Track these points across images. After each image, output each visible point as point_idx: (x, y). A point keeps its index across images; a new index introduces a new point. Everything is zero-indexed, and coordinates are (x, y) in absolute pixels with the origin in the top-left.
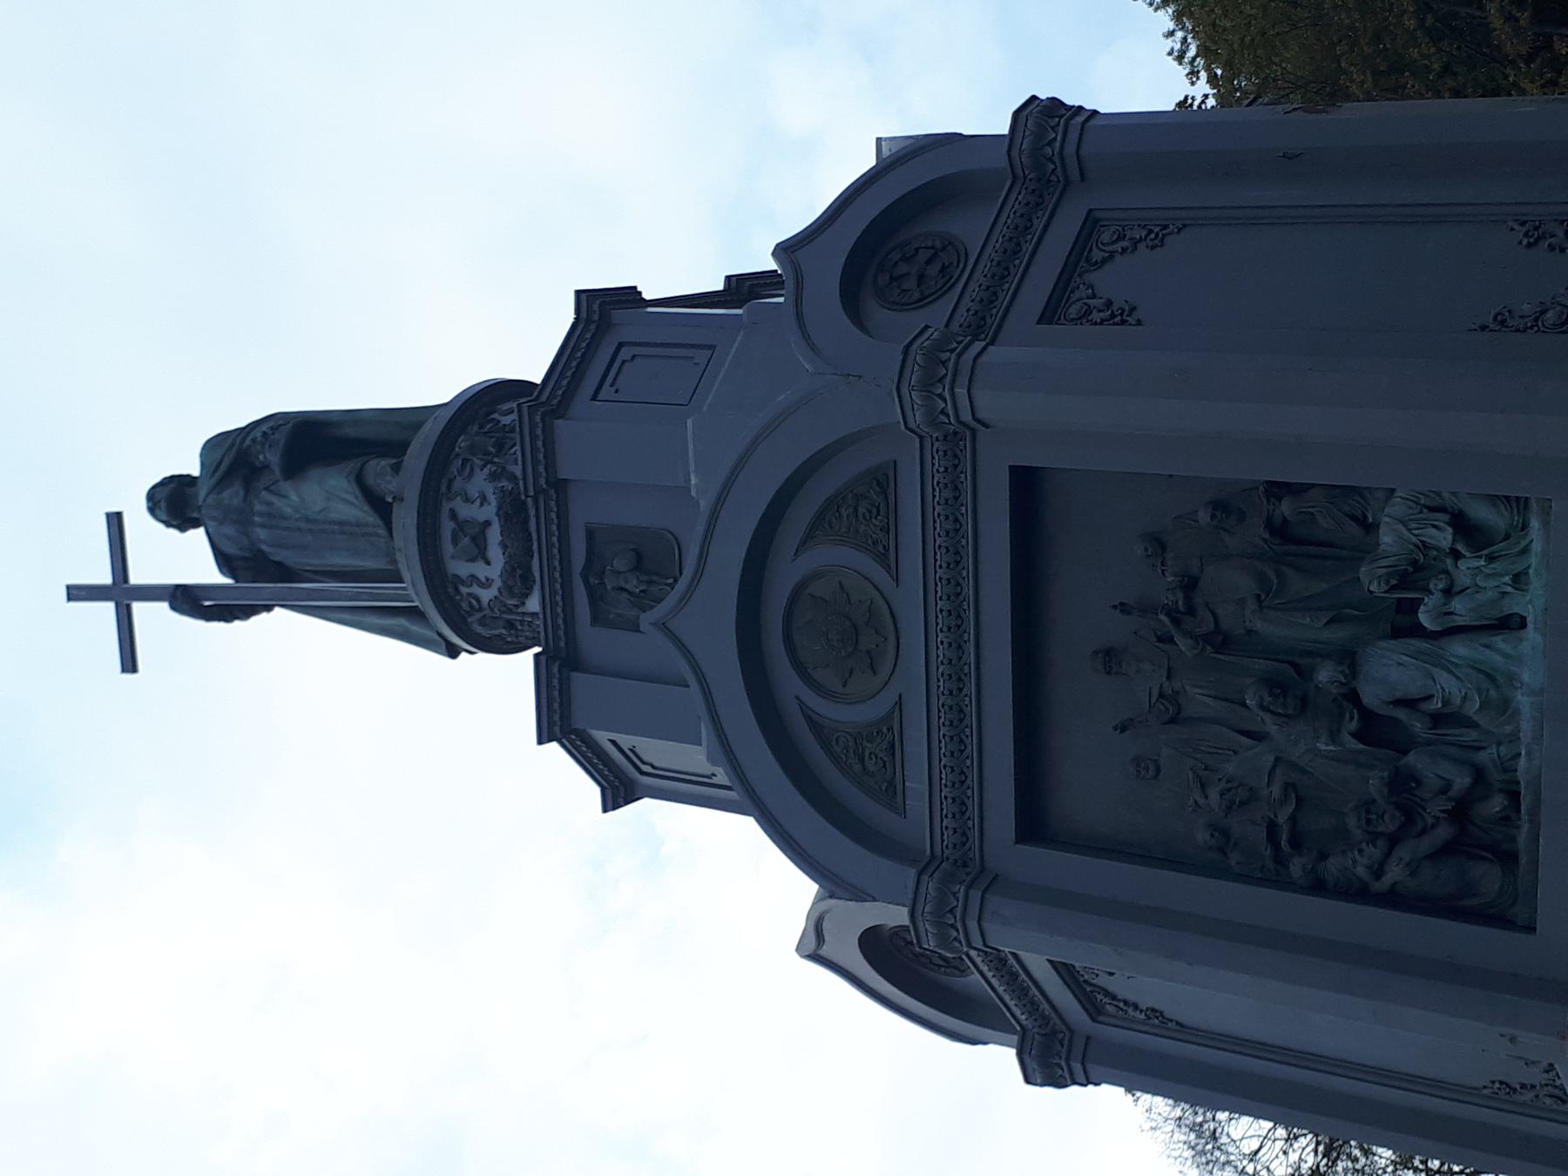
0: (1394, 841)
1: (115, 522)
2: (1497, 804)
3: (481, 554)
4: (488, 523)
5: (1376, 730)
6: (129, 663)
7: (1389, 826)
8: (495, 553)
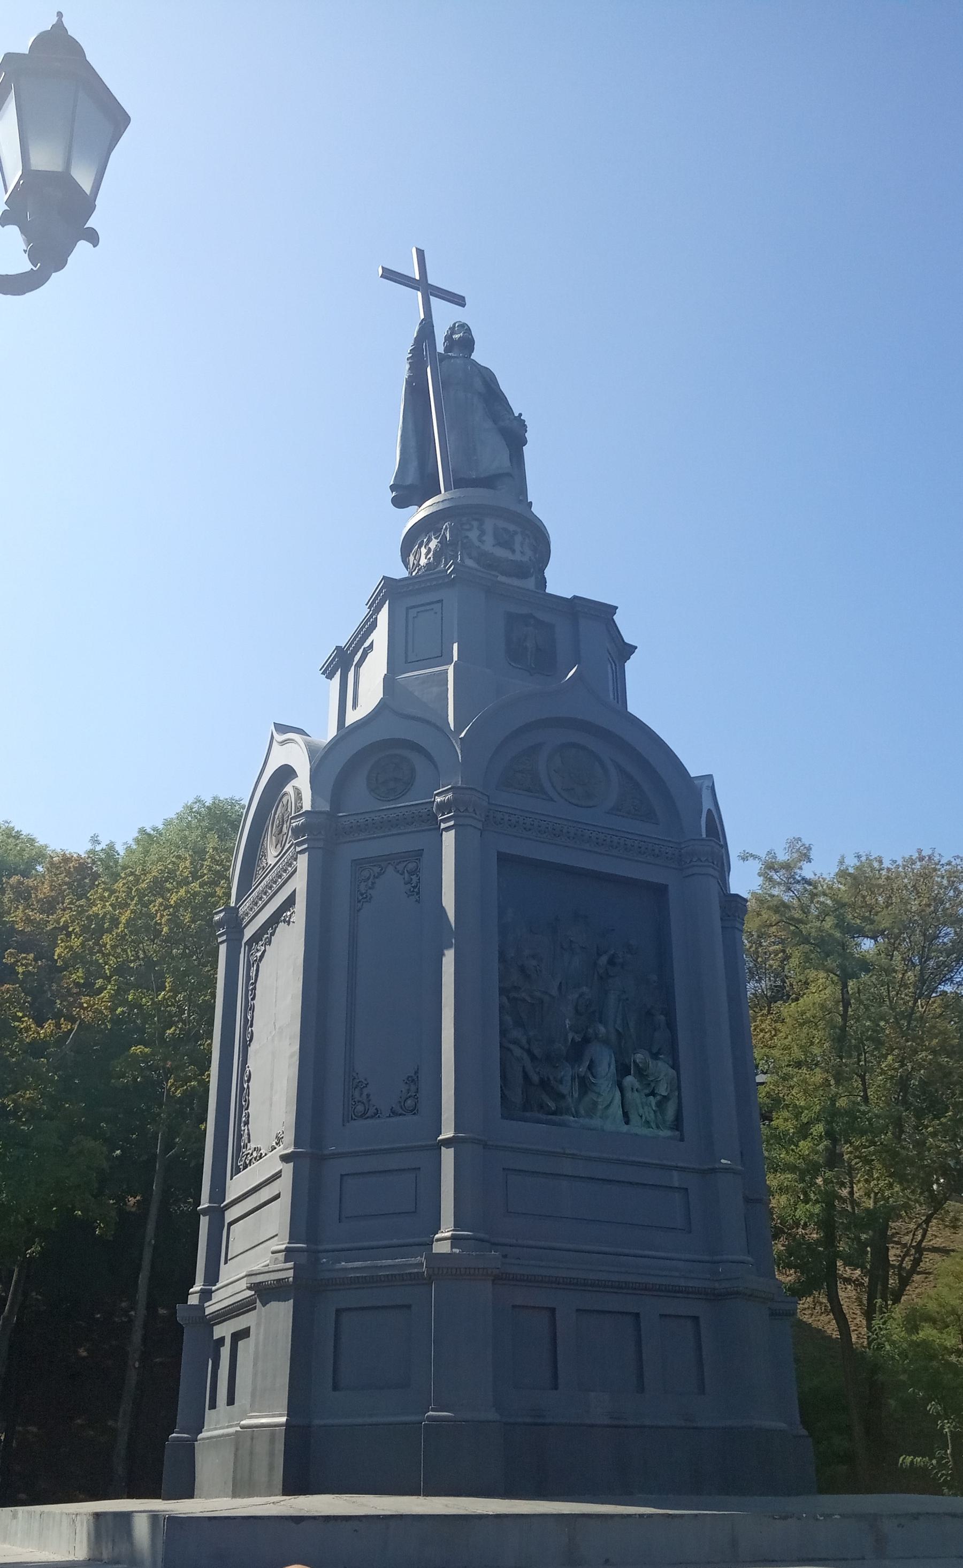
0: (529, 1052)
1: (459, 301)
2: (552, 1105)
3: (499, 543)
4: (514, 551)
5: (577, 1051)
6: (389, 274)
7: (537, 1052)
8: (501, 553)
